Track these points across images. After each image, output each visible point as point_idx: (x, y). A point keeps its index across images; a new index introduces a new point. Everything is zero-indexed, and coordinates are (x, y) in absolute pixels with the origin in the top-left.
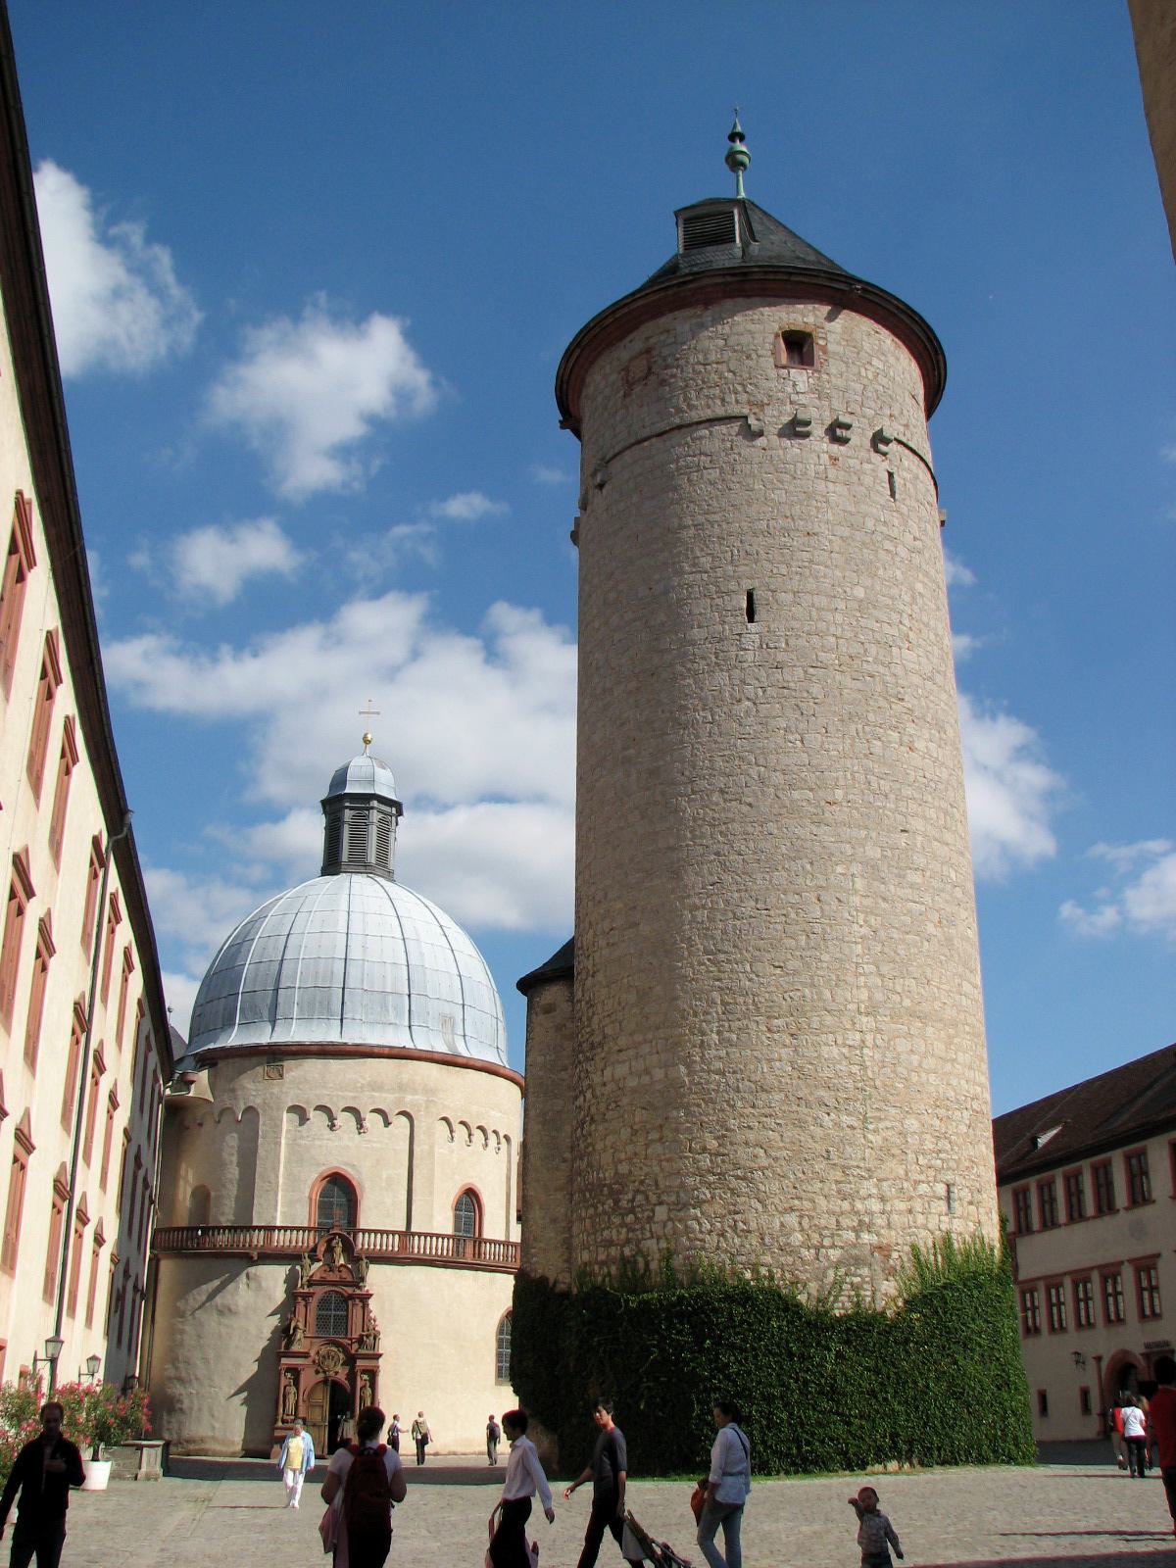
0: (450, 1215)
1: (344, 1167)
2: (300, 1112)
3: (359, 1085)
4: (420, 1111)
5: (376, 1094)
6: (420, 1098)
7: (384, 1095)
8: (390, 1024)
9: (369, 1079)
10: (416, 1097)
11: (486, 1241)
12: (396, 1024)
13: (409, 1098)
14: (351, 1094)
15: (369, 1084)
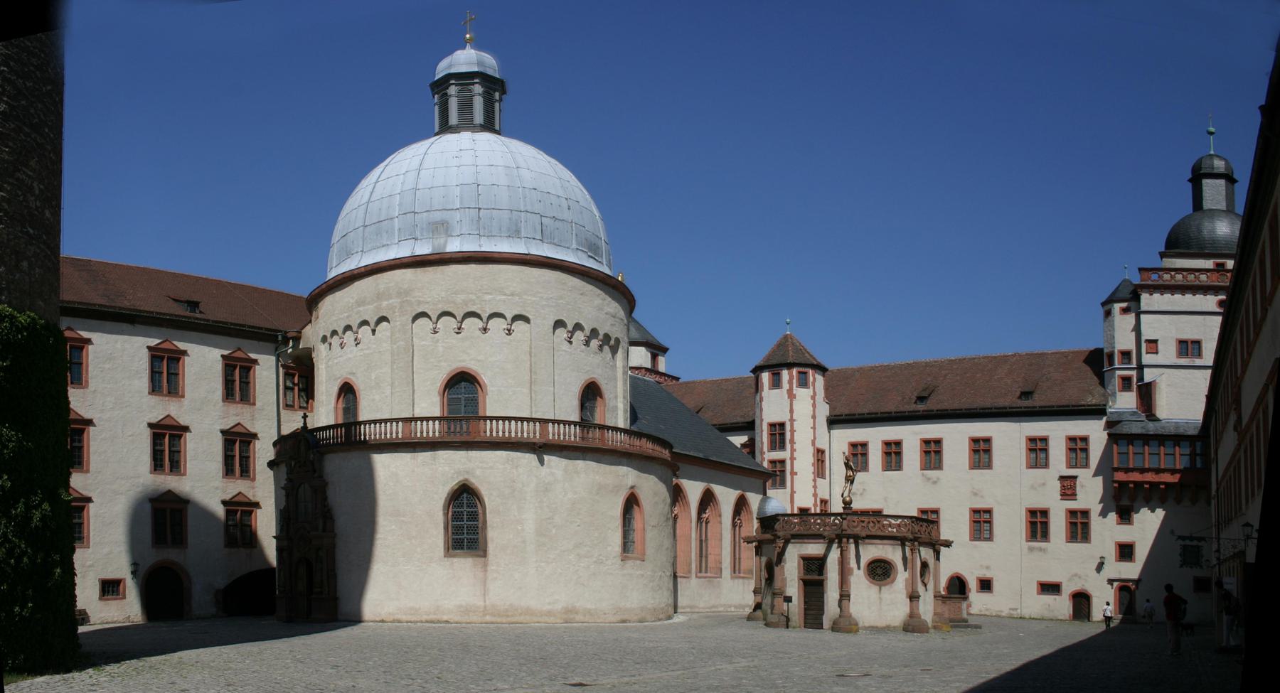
0: (437, 399)
1: (349, 376)
2: (324, 339)
3: (350, 305)
4: (395, 312)
5: (361, 309)
6: (395, 301)
7: (366, 307)
8: (383, 246)
9: (356, 298)
10: (391, 301)
11: (485, 418)
12: (388, 245)
13: (385, 303)
14: (346, 315)
15: (357, 302)
